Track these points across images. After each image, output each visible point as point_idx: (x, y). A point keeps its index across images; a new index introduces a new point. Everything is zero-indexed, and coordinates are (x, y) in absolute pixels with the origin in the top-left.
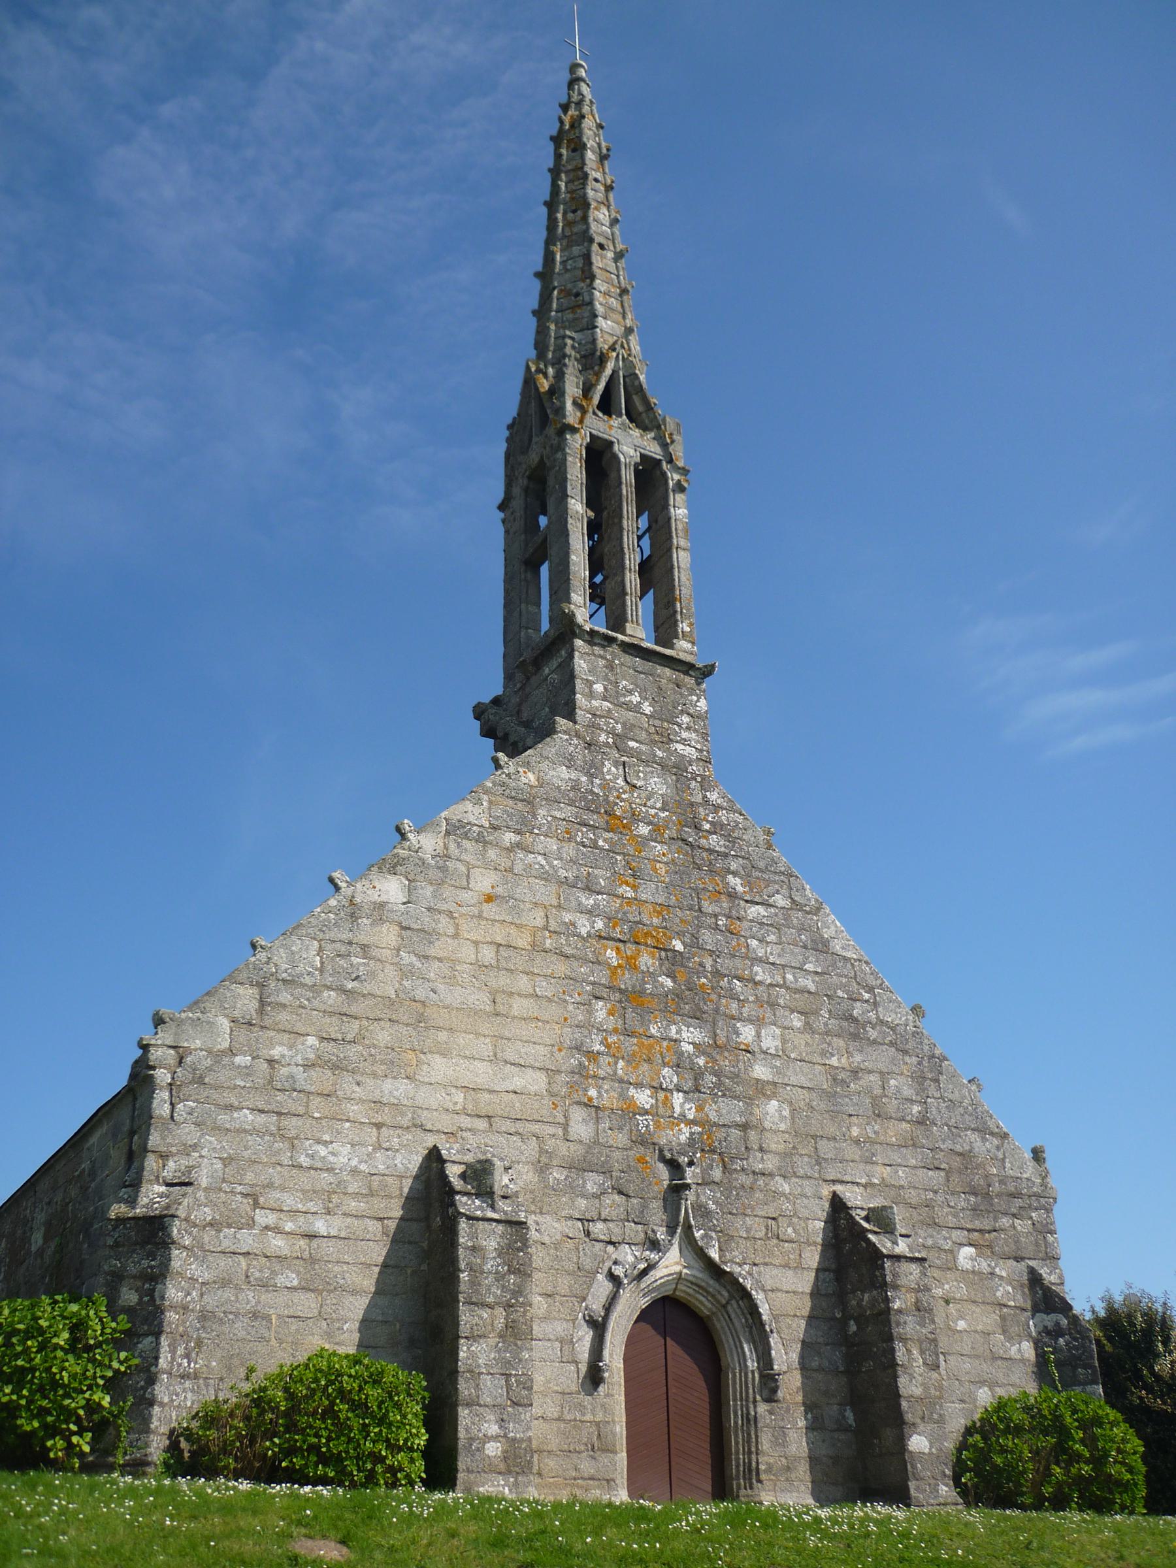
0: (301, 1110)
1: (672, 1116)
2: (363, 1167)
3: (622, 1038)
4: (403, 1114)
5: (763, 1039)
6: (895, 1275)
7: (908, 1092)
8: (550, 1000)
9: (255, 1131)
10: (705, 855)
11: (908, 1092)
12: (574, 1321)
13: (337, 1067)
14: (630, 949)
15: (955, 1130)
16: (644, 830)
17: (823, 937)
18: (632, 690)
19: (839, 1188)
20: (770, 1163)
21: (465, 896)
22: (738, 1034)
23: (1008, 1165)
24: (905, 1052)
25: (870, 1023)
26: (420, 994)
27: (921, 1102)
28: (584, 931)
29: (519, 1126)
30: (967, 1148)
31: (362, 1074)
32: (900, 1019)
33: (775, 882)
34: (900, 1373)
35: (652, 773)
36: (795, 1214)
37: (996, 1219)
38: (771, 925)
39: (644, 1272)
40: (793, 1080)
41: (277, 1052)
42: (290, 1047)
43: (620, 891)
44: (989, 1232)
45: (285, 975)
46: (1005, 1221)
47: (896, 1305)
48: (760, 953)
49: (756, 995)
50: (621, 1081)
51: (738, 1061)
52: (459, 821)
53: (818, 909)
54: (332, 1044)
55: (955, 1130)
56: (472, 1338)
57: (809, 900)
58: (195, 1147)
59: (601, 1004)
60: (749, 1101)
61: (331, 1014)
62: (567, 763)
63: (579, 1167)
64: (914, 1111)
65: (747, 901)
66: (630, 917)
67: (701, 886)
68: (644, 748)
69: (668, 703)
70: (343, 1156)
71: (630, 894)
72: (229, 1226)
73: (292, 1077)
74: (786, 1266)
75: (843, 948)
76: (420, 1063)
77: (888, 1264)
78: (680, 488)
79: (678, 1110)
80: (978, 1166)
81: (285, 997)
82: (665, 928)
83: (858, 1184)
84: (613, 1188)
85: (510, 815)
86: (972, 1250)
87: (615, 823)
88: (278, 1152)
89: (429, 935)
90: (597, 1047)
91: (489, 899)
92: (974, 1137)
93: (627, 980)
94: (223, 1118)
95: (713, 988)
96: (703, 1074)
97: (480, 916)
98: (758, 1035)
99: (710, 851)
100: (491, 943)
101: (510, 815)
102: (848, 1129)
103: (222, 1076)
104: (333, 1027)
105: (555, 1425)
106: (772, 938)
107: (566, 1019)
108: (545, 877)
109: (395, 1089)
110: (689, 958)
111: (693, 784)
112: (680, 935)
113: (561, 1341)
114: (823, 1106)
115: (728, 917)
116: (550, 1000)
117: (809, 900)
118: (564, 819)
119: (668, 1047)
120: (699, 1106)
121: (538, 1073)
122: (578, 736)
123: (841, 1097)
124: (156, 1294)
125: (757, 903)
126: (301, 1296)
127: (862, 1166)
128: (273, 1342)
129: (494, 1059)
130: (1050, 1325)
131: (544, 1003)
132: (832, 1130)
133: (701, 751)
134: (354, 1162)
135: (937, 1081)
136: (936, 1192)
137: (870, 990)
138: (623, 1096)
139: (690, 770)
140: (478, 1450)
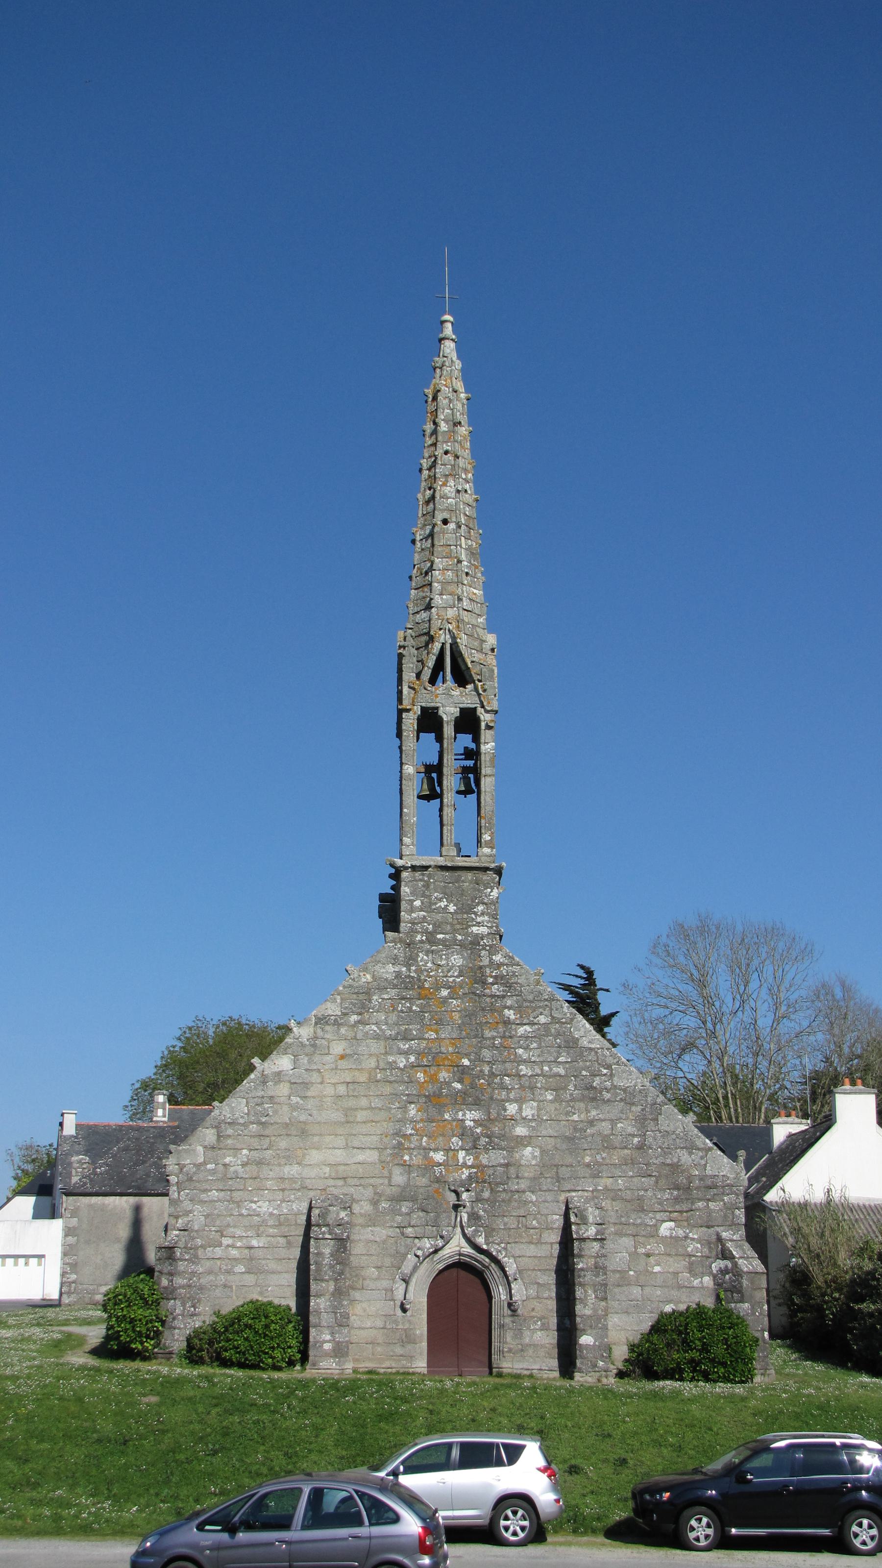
0: (242, 1187)
1: (458, 1165)
2: (275, 1212)
3: (426, 1124)
4: (296, 1183)
5: (524, 1111)
8: (380, 1109)
9: (219, 1200)
10: (488, 1000)
11: (630, 1130)
12: (393, 1280)
13: (260, 1163)
14: (433, 1070)
15: (666, 1151)
16: (445, 993)
17: (573, 1038)
18: (441, 898)
21: (328, 1058)
22: (505, 1110)
23: (708, 1168)
24: (633, 1104)
25: (606, 1089)
26: (303, 1118)
27: (640, 1135)
28: (402, 1065)
29: (362, 1181)
30: (675, 1160)
31: (273, 1165)
32: (631, 1082)
33: (540, 1007)
34: (577, 1303)
35: (453, 952)
36: (539, 1212)
37: (693, 1203)
38: (535, 1037)
39: (436, 1251)
40: (544, 1133)
41: (228, 1160)
42: (234, 1157)
43: (427, 1036)
44: (686, 1212)
45: (229, 1120)
46: (700, 1204)
49: (521, 1084)
50: (425, 1149)
51: (505, 1127)
52: (323, 1015)
53: (572, 1020)
54: (256, 1151)
55: (666, 1151)
56: (318, 1296)
57: (566, 1014)
58: (191, 1212)
59: (413, 1106)
60: (510, 1150)
61: (254, 1136)
62: (393, 961)
64: (634, 1142)
65: (518, 1024)
66: (434, 1050)
67: (484, 1021)
68: (447, 937)
69: (468, 900)
70: (264, 1207)
71: (433, 1035)
72: (210, 1247)
73: (236, 1172)
74: (531, 1243)
75: (589, 1042)
76: (304, 1155)
78: (489, 727)
79: (461, 1161)
80: (683, 1172)
81: (230, 1131)
82: (458, 1052)
83: (587, 1191)
84: (418, 1209)
85: (354, 1005)
86: (672, 1224)
88: (231, 1209)
89: (306, 1085)
90: (410, 1132)
93: (430, 1089)
94: (203, 1196)
95: (489, 1084)
96: (479, 1138)
97: (336, 1069)
99: (492, 996)
100: (343, 1083)
101: (354, 1005)
102: (583, 1158)
103: (201, 1176)
104: (255, 1142)
105: (381, 1331)
106: (535, 1045)
107: (390, 1118)
108: (377, 1037)
109: (292, 1170)
110: (473, 1069)
111: (483, 953)
112: (467, 1055)
113: (386, 1290)
114: (564, 1146)
116: (380, 1109)
117: (566, 1014)
118: (390, 999)
119: (456, 1126)
120: (476, 1157)
121: (373, 1151)
122: (401, 941)
123: (579, 1139)
125: (525, 1024)
126: (247, 1276)
127: (590, 1180)
128: (234, 1297)
129: (346, 1147)
130: (722, 1266)
131: (377, 1111)
132: (569, 1160)
133: (491, 927)
134: (271, 1210)
137: (609, 1067)
138: (426, 1157)
139: (482, 943)
140: (320, 1346)
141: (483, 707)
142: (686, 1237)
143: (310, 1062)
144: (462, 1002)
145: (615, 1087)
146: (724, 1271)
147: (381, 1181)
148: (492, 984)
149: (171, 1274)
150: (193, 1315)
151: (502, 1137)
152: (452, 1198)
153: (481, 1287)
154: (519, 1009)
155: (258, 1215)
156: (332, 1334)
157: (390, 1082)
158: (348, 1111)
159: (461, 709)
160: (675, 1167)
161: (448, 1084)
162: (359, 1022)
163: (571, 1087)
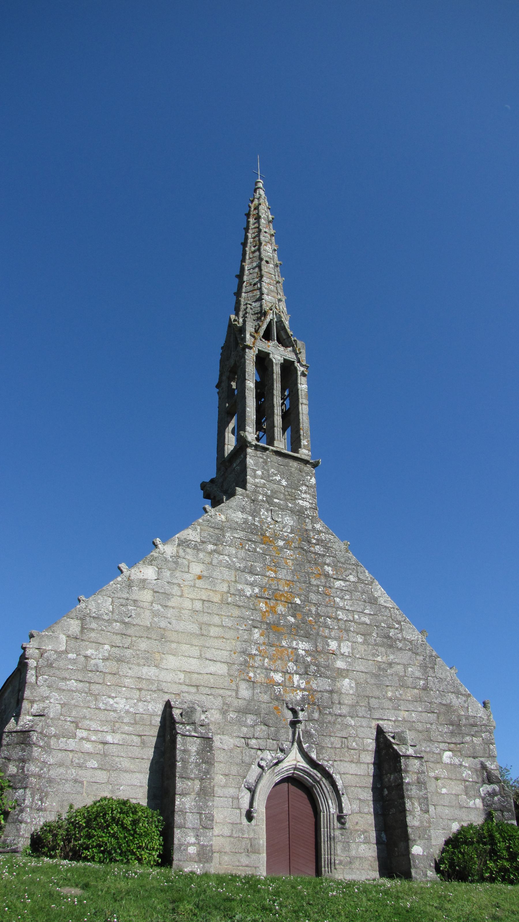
0: (101, 681)
1: (293, 687)
2: (132, 710)
3: (267, 647)
4: (152, 684)
5: (342, 648)
6: (406, 765)
7: (418, 674)
8: (230, 628)
10: (313, 555)
11: (418, 674)
12: (239, 788)
13: (120, 660)
14: (272, 603)
16: (281, 543)
17: (374, 596)
18: (276, 474)
19: (381, 722)
20: (345, 710)
21: (186, 576)
22: (328, 645)
23: (470, 710)
24: (417, 654)
25: (399, 639)
26: (163, 624)
27: (424, 679)
28: (248, 594)
29: (213, 691)
30: (449, 702)
31: (132, 664)
32: (414, 637)
33: (349, 569)
34: (408, 814)
35: (286, 514)
36: (357, 735)
37: (463, 737)
38: (347, 591)
39: (277, 764)
40: (357, 668)
41: (89, 652)
42: (97, 650)
43: (268, 574)
44: (459, 744)
45: (94, 614)
46: (468, 739)
47: (407, 780)
48: (341, 604)
49: (339, 626)
50: (266, 669)
51: (328, 659)
52: (185, 539)
53: (372, 582)
54: (117, 649)
55: (442, 693)
56: (183, 795)
57: (367, 578)
58: (47, 698)
59: (257, 630)
60: (334, 679)
61: (117, 634)
62: (242, 510)
63: (244, 711)
64: (421, 684)
65: (334, 578)
66: (273, 587)
67: (311, 571)
68: (282, 502)
69: (295, 480)
70: (121, 704)
71: (273, 575)
72: (64, 737)
73: (96, 665)
74: (352, 762)
75: (385, 602)
76: (162, 659)
77: (403, 760)
79: (296, 683)
80: (454, 711)
81: (94, 625)
82: (291, 592)
83: (390, 720)
84: (261, 722)
85: (211, 536)
87: (265, 540)
88: (89, 701)
89: (168, 595)
90: (254, 652)
91: (200, 577)
92: (452, 696)
93: (270, 618)
94: (62, 684)
95: (315, 622)
96: (310, 665)
97: (194, 586)
98: (339, 646)
100: (200, 599)
101: (211, 536)
102: (386, 693)
104: (117, 640)
105: (228, 839)
106: (347, 597)
107: (238, 638)
108: (229, 567)
110: (303, 607)
111: (307, 520)
112: (299, 595)
113: (233, 798)
114: (373, 681)
115: (324, 586)
116: (230, 628)
117: (367, 578)
118: (239, 538)
119: (292, 653)
120: (308, 681)
121: (223, 665)
122: (247, 496)
123: (383, 677)
124: (25, 769)
125: (340, 580)
126: (99, 772)
127: (393, 711)
128: (85, 794)
129: (200, 657)
131: (227, 630)
132: (377, 693)
133: (312, 504)
134: (127, 707)
135: (433, 668)
136: (431, 724)
137: (399, 623)
138: (267, 676)
139: (306, 513)
140: (184, 850)
141: (299, 362)
142: (461, 765)
143: (172, 575)
144: (294, 553)
145: (405, 639)
146: (492, 794)
147: (229, 693)
148: (316, 544)
149: (23, 761)
150: (39, 810)
151: (327, 667)
152: (289, 716)
153: (307, 801)
154: (335, 567)
155: (115, 711)
156: (197, 836)
157: (239, 606)
158: (201, 625)
159: (285, 359)
160: (449, 706)
161: (285, 616)
162: (215, 551)
163: (374, 634)
